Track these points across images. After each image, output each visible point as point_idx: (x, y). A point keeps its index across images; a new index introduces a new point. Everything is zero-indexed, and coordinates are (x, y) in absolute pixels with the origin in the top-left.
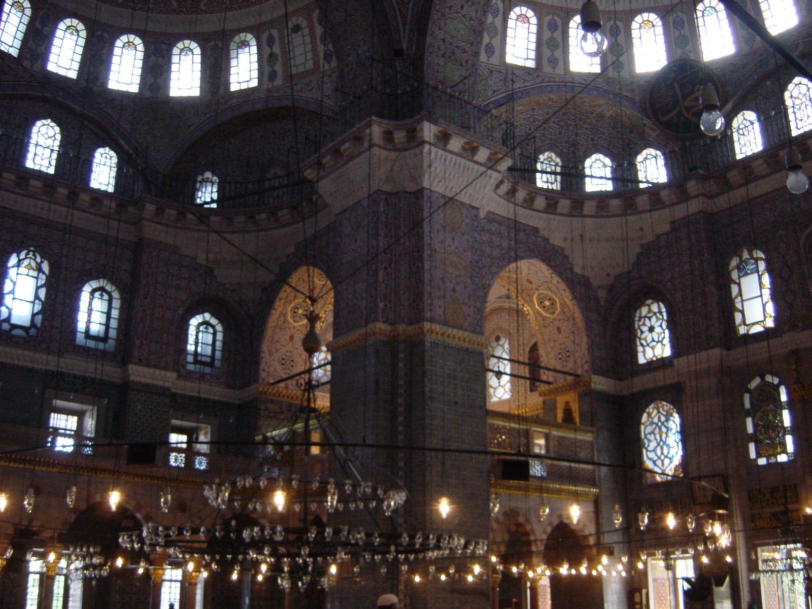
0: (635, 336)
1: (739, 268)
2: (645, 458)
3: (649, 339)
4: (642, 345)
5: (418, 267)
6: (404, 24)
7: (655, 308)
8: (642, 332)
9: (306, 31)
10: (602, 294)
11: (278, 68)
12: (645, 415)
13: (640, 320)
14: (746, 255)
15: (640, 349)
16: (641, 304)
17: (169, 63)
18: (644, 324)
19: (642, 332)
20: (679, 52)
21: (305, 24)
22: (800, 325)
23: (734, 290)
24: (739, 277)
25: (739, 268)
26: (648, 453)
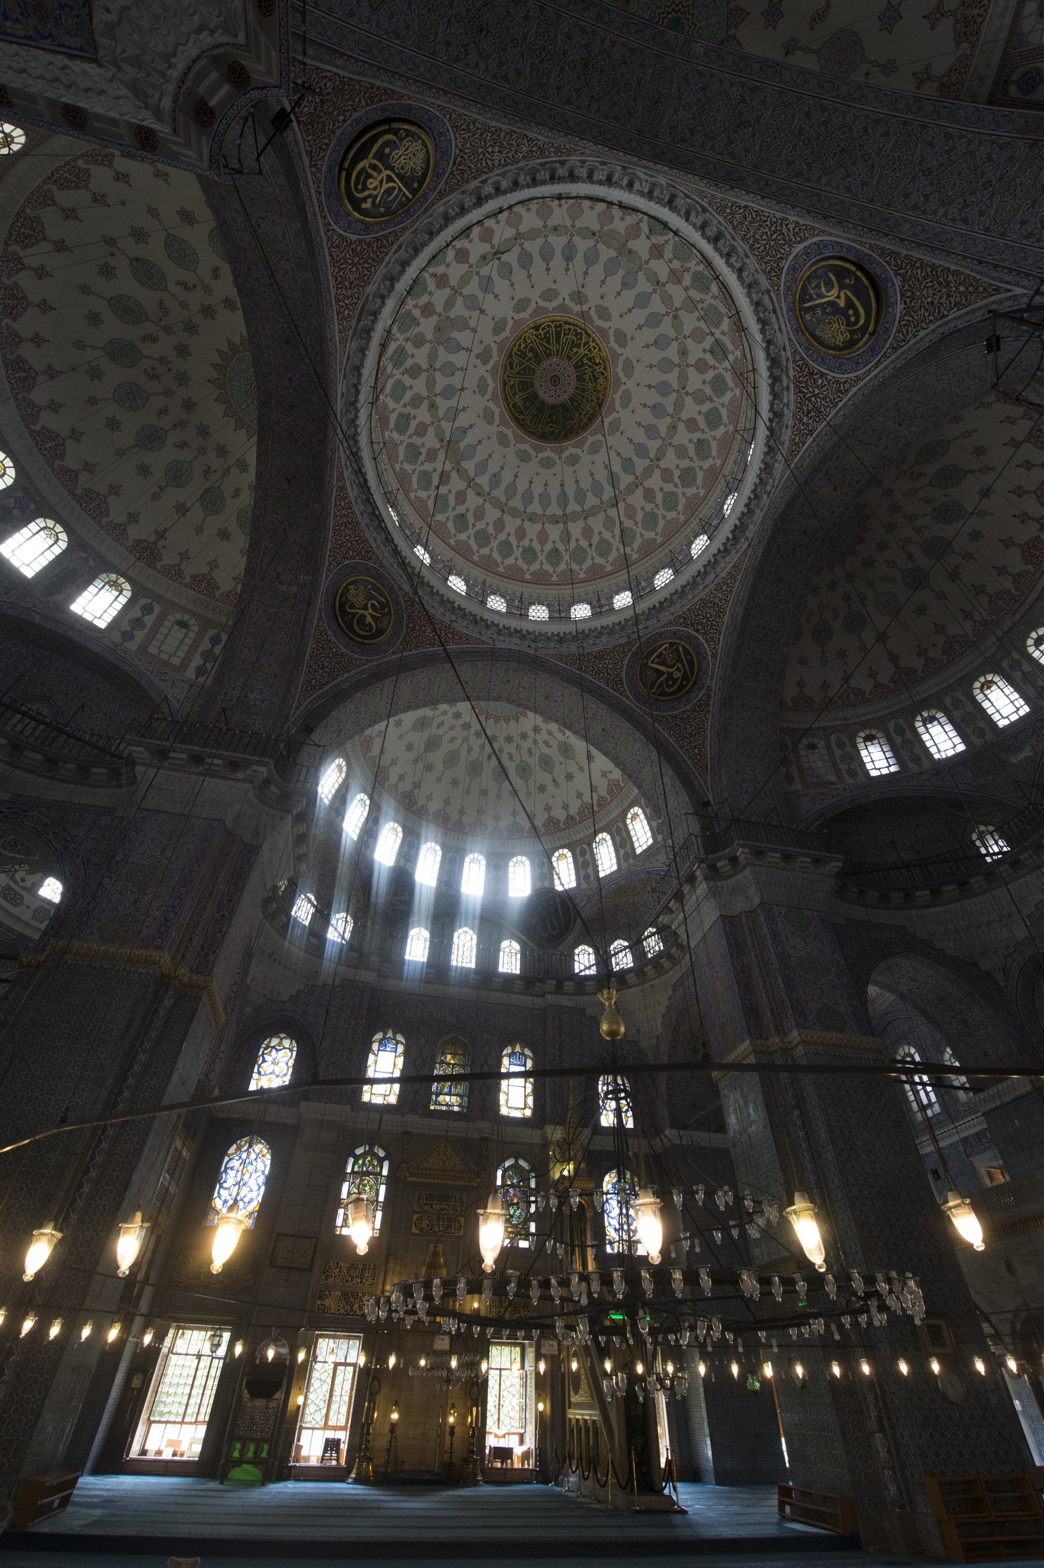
0: (256, 1062)
1: (381, 1042)
2: (216, 1194)
3: (269, 1070)
4: (259, 1073)
5: (223, 916)
6: (297, 708)
7: (287, 1043)
8: (264, 1061)
9: (192, 635)
10: (248, 1010)
11: (140, 636)
12: (234, 1147)
13: (266, 1049)
14: (390, 1034)
15: (255, 1076)
16: (274, 1034)
17: (25, 522)
18: (270, 1054)
19: (264, 1061)
20: (402, 863)
21: (196, 629)
22: (420, 1111)
23: (371, 1058)
24: (379, 1050)
25: (381, 1042)
26: (222, 1191)
